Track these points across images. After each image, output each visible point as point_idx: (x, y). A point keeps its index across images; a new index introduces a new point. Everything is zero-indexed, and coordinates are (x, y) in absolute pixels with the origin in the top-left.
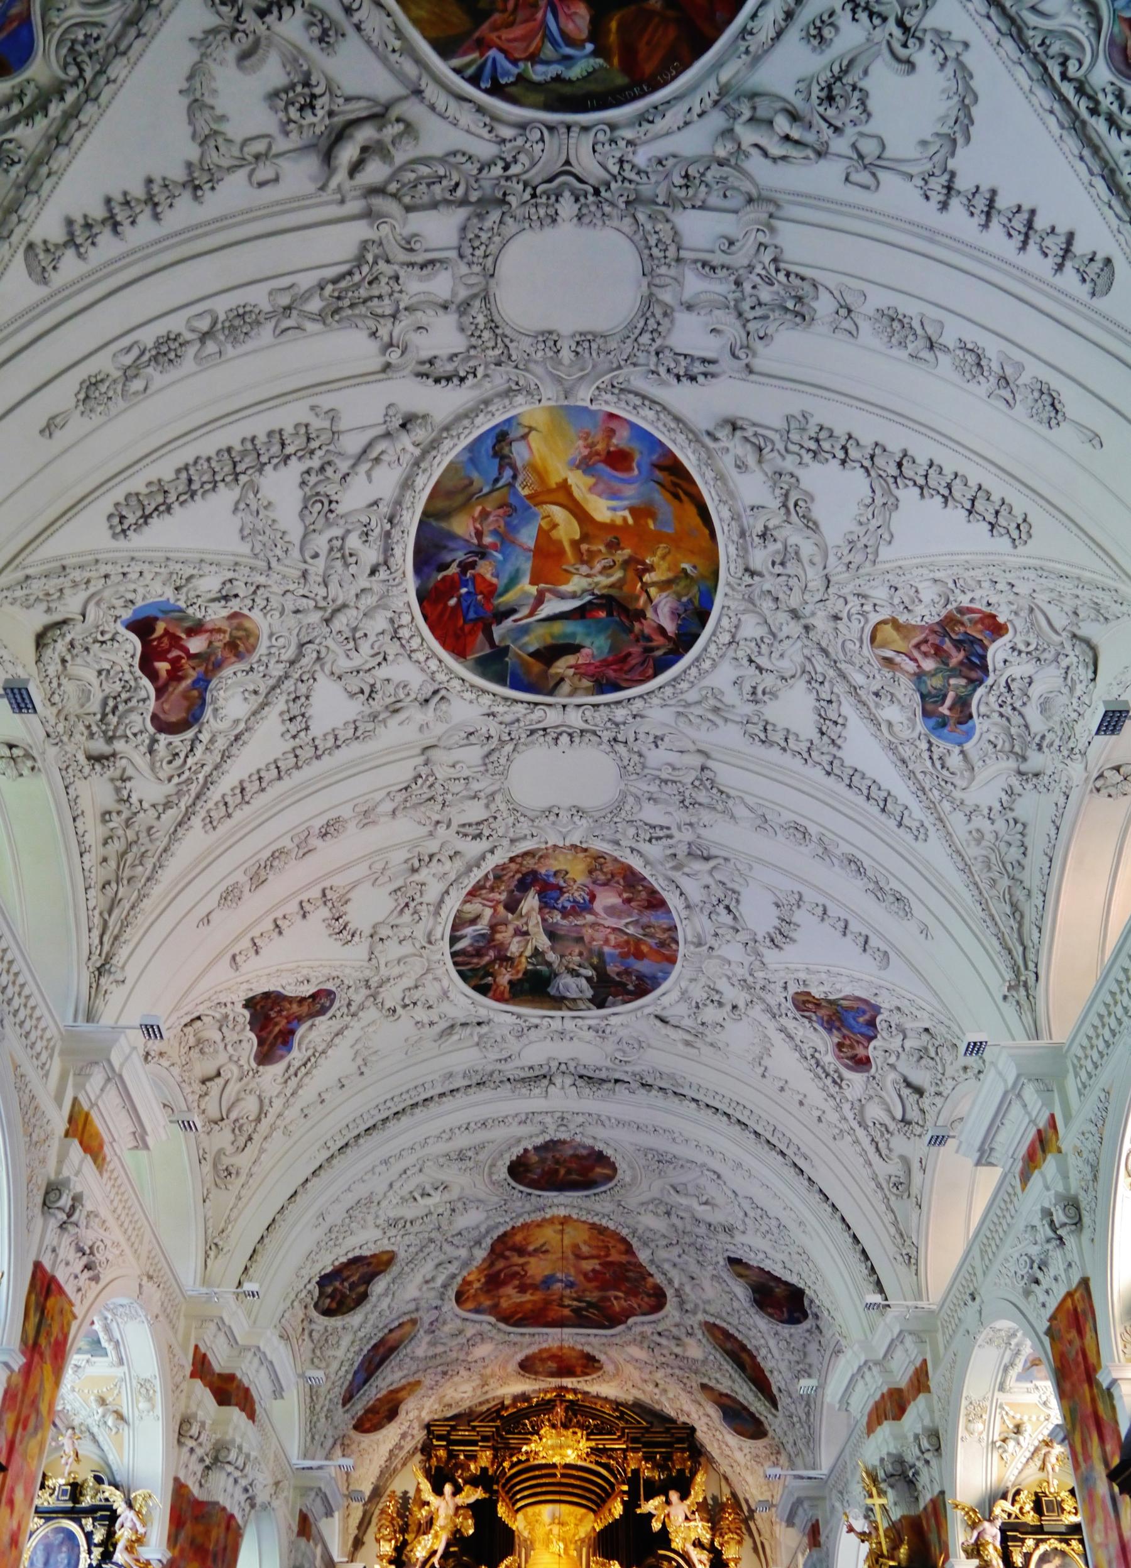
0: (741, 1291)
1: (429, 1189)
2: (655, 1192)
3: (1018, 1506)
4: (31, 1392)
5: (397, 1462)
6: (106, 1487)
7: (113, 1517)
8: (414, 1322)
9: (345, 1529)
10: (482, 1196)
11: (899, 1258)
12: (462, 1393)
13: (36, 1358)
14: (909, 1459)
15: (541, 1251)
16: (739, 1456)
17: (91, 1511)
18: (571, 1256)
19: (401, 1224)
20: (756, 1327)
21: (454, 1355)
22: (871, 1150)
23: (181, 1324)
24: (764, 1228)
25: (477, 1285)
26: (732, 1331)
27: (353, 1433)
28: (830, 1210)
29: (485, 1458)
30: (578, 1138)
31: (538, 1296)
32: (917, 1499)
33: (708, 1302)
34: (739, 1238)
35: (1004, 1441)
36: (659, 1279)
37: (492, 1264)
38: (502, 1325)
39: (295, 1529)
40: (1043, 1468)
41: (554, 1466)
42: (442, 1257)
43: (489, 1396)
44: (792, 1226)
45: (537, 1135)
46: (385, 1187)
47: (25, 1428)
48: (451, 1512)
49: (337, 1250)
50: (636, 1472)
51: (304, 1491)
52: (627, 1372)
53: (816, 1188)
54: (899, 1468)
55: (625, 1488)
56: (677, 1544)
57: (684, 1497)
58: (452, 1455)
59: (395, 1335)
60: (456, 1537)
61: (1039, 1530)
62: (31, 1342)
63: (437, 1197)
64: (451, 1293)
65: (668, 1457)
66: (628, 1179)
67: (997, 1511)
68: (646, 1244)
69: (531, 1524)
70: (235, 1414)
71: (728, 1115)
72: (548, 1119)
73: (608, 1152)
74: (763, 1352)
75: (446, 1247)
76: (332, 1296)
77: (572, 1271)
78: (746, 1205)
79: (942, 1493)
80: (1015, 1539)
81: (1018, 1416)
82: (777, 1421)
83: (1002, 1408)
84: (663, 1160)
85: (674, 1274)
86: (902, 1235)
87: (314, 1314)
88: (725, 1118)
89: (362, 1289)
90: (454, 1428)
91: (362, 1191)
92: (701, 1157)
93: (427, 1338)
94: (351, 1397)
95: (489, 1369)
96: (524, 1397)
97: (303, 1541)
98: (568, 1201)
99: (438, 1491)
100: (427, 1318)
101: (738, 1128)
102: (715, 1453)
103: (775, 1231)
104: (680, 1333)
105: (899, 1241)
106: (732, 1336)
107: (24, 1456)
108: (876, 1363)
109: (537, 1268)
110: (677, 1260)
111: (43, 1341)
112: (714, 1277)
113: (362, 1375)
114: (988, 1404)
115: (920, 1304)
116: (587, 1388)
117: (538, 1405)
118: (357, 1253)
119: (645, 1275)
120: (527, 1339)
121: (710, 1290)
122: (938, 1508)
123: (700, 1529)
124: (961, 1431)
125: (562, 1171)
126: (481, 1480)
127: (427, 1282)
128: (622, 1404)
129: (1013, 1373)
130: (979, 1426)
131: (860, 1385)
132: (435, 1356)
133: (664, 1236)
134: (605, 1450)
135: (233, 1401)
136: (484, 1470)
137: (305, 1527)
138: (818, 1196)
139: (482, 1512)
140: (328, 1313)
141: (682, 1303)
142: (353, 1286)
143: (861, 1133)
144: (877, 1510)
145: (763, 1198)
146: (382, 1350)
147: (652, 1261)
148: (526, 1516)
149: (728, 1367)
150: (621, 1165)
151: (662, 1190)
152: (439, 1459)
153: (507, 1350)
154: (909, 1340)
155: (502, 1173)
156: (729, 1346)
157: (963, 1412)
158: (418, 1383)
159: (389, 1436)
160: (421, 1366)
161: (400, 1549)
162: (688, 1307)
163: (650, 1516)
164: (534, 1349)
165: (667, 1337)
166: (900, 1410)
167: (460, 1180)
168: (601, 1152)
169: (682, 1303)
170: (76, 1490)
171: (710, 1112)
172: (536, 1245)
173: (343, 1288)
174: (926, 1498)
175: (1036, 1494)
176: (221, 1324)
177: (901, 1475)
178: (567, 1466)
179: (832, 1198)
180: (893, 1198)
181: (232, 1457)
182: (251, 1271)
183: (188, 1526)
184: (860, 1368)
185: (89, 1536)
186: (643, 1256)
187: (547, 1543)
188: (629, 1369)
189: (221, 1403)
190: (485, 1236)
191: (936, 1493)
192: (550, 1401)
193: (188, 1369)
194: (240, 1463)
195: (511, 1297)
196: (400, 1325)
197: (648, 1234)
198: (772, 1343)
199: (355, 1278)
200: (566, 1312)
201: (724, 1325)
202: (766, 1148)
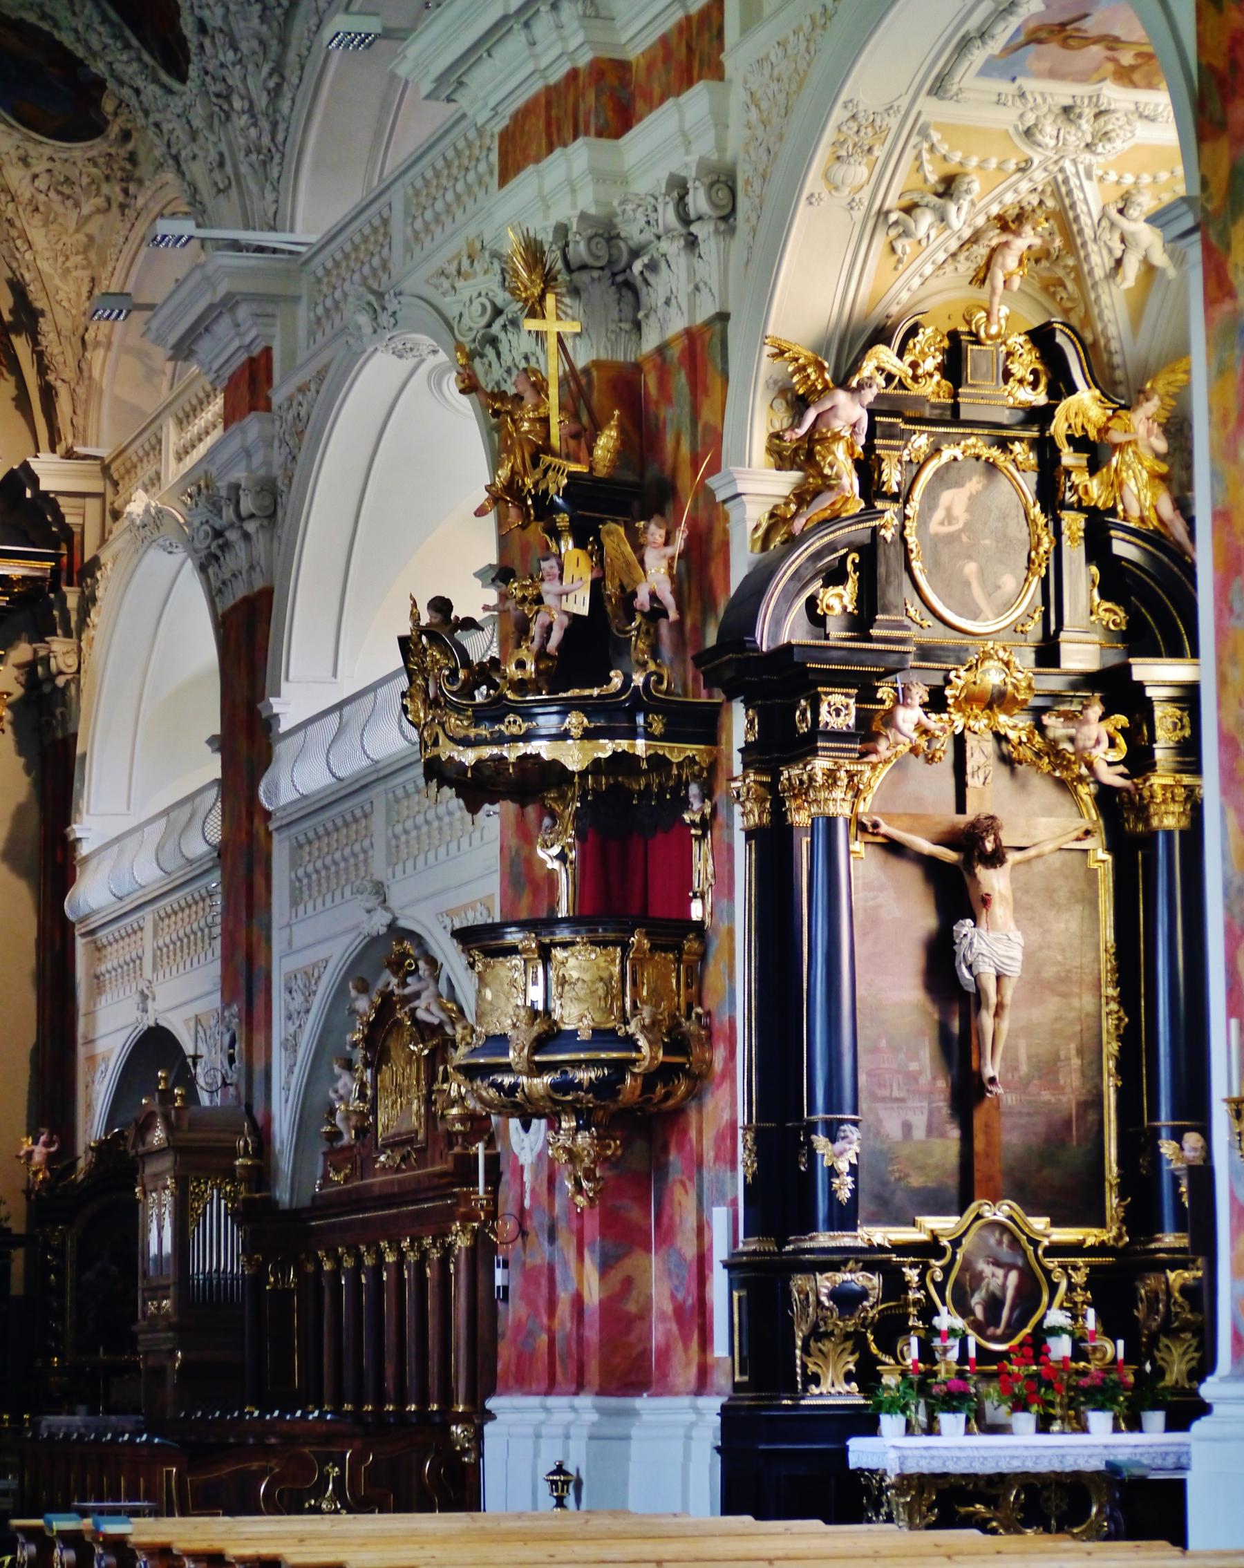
3: (908, 358)
14: (633, 231)
32: (638, 326)
35: (909, 210)
40: (982, 277)
54: (602, 251)
61: (952, 416)
67: (868, 368)
79: (723, 317)
80: (891, 432)
81: (957, 157)
82: (177, 105)
83: (924, 134)
114: (893, 122)
122: (703, 355)
124: (813, 182)
129: (978, 56)
130: (859, 172)
131: (515, 43)
144: (552, 342)
157: (829, 135)
166: (620, 120)
174: (666, 324)
175: (953, 335)
177: (606, 269)
191: (702, 316)
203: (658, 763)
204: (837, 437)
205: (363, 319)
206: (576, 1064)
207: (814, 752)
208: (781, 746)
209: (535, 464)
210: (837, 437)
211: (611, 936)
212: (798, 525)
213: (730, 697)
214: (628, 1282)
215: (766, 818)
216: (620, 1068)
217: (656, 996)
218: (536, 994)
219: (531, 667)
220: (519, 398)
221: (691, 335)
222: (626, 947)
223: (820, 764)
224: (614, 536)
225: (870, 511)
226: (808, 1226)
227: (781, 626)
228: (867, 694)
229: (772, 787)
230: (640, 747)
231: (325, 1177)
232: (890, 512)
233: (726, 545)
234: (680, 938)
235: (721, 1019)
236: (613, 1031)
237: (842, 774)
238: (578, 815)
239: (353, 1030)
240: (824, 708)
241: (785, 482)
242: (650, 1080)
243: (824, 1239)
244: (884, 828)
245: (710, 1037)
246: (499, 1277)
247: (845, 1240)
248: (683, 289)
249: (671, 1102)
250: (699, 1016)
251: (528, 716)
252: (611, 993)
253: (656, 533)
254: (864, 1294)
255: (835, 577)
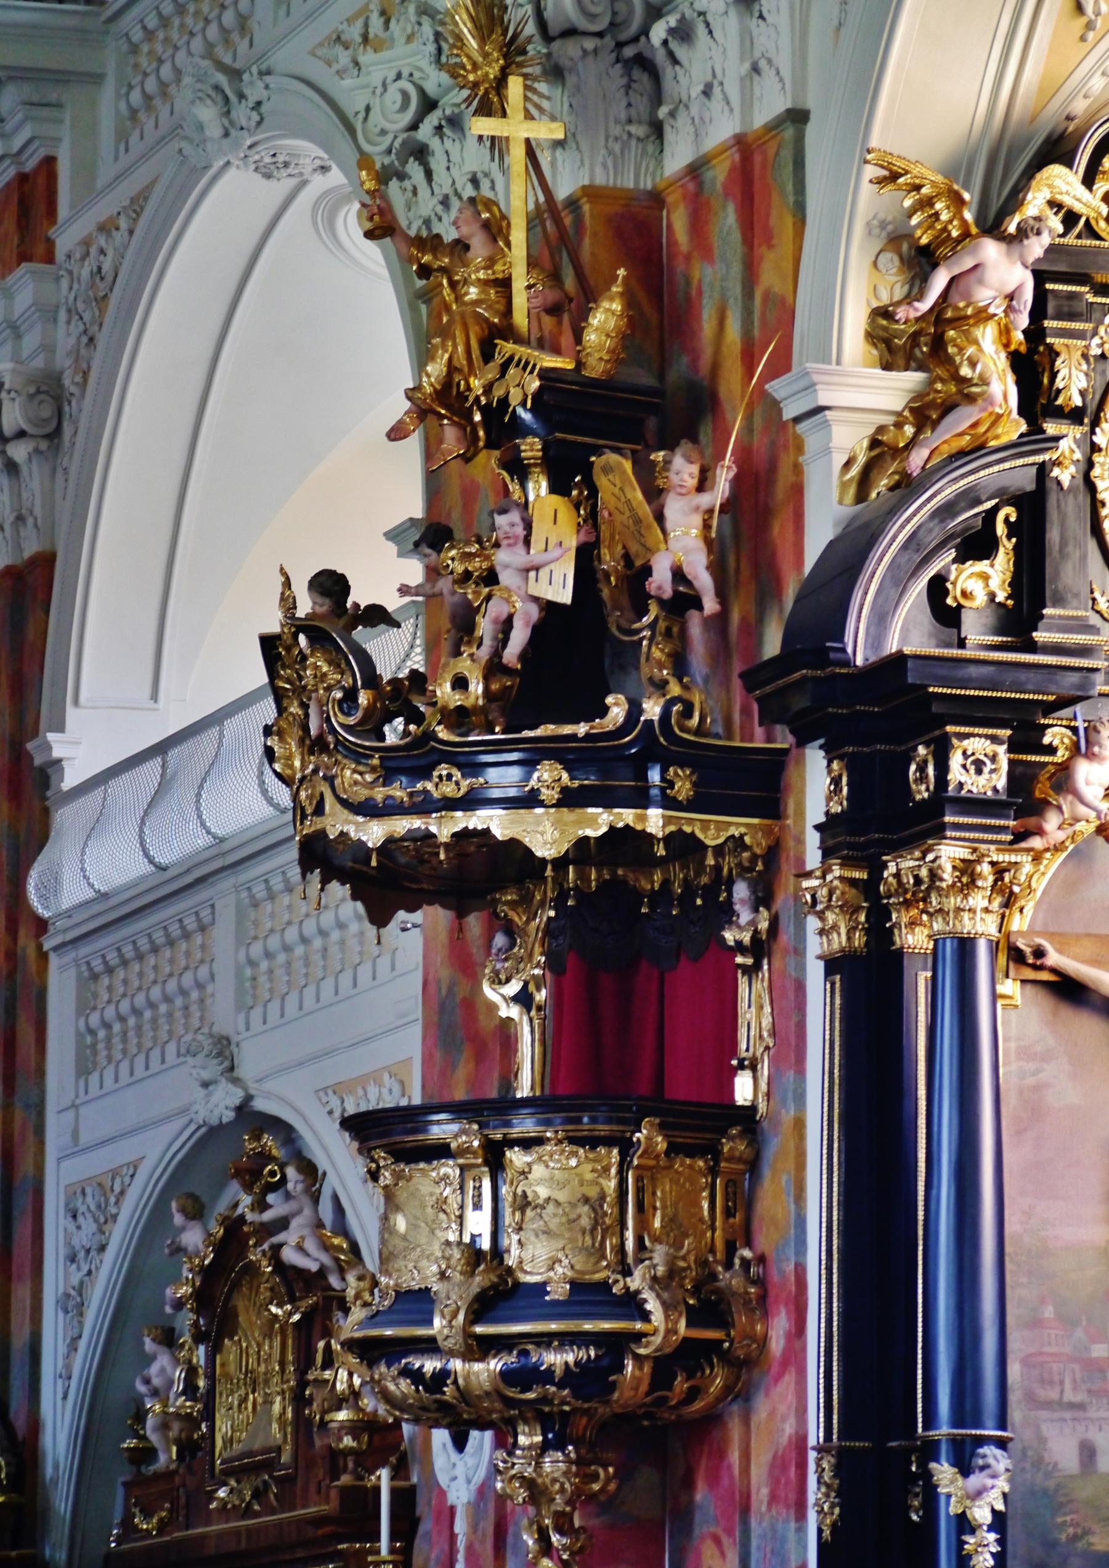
32: (657, 130)
67: (1035, 203)
79: (798, 117)
122: (763, 176)
144: (517, 154)
174: (704, 130)
203: (683, 846)
204: (983, 316)
205: (208, 114)
206: (544, 1340)
207: (939, 832)
208: (885, 820)
209: (487, 355)
210: (983, 316)
211: (603, 1129)
212: (917, 460)
213: (802, 741)
215: (859, 940)
216: (615, 1347)
217: (675, 1230)
218: (479, 1223)
219: (477, 688)
220: (461, 246)
221: (745, 146)
222: (626, 1147)
223: (949, 853)
224: (615, 473)
225: (1035, 437)
227: (886, 626)
228: (1026, 738)
229: (869, 889)
230: (654, 820)
231: (127, 1523)
232: (1069, 440)
233: (798, 491)
234: (718, 1135)
235: (782, 1269)
236: (604, 1286)
237: (985, 868)
238: (550, 931)
239: (176, 1280)
240: (956, 760)
241: (896, 389)
242: (663, 1367)
244: (1053, 958)
245: (763, 1297)
248: (733, 70)
249: (698, 1405)
250: (746, 1264)
251: (472, 768)
252: (601, 1221)
253: (683, 469)
255: (977, 545)
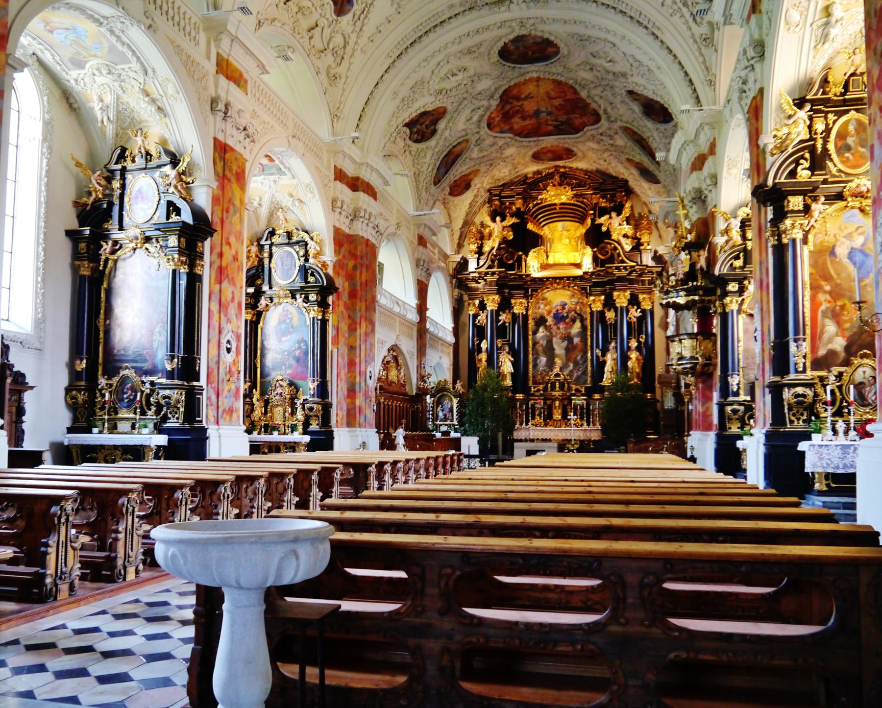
0: (636, 108)
1: (455, 71)
2: (582, 58)
4: (227, 197)
5: (475, 209)
6: (301, 232)
7: (306, 244)
8: (467, 141)
9: (452, 240)
10: (489, 72)
11: (705, 83)
12: (503, 173)
13: (226, 181)
15: (528, 97)
16: (649, 192)
17: (297, 243)
18: (547, 99)
19: (444, 93)
20: (646, 126)
21: (494, 155)
22: (691, 20)
23: (325, 156)
24: (642, 72)
25: (498, 119)
26: (635, 130)
27: (449, 197)
28: (673, 58)
29: (519, 203)
30: (533, 33)
31: (533, 121)
32: (706, 209)
33: (621, 116)
34: (631, 79)
36: (594, 106)
37: (503, 107)
38: (517, 138)
39: (416, 242)
41: (555, 204)
42: (473, 107)
43: (519, 173)
44: (655, 69)
45: (510, 34)
46: (430, 73)
47: (228, 212)
48: (501, 229)
49: (410, 110)
50: (596, 204)
51: (419, 226)
52: (589, 156)
53: (665, 46)
55: (592, 212)
56: (614, 236)
57: (619, 214)
58: (502, 203)
59: (458, 149)
60: (504, 240)
62: (221, 175)
63: (461, 76)
64: (484, 124)
65: (613, 196)
66: (566, 53)
68: (584, 88)
69: (552, 232)
70: (361, 195)
71: (614, 8)
72: (514, 24)
73: (552, 38)
74: (651, 139)
75: (474, 101)
76: (418, 132)
77: (549, 106)
78: (631, 60)
84: (583, 40)
85: (601, 102)
86: (707, 69)
87: (410, 143)
88: (613, 11)
89: (432, 128)
90: (502, 190)
91: (416, 77)
92: (603, 35)
93: (476, 149)
94: (439, 181)
95: (516, 160)
96: (538, 172)
97: (421, 248)
98: (536, 69)
99: (494, 221)
100: (473, 139)
101: (620, 15)
102: (639, 192)
103: (647, 73)
104: (612, 132)
105: (706, 73)
106: (635, 133)
107: (231, 223)
108: (691, 142)
109: (530, 106)
110: (602, 94)
111: (228, 173)
112: (622, 102)
113: (442, 170)
115: (714, 107)
116: (570, 165)
117: (546, 175)
118: (423, 110)
119: (587, 105)
120: (532, 144)
121: (622, 109)
122: (713, 216)
123: (628, 229)
125: (530, 53)
126: (518, 214)
127: (468, 120)
128: (591, 172)
131: (684, 154)
132: (484, 157)
133: (592, 82)
134: (581, 195)
135: (361, 189)
136: (518, 209)
137: (422, 241)
138: (666, 51)
139: (519, 229)
140: (417, 141)
141: (608, 118)
142: (427, 127)
143: (684, 10)
145: (640, 56)
146: (452, 157)
147: (588, 96)
148: (549, 228)
149: (637, 149)
150: (561, 45)
151: (586, 56)
152: (496, 205)
153: (523, 151)
154: (706, 128)
155: (495, 57)
156: (636, 137)
157: (725, 164)
158: (478, 170)
159: (467, 198)
160: (478, 162)
161: (480, 247)
162: (612, 119)
163: (601, 225)
164: (539, 148)
165: (606, 136)
167: (473, 65)
168: (547, 39)
169: (608, 118)
170: (289, 235)
171: (604, 7)
172: (526, 94)
173: (422, 127)
176: (345, 155)
178: (562, 204)
179: (675, 51)
180: (703, 48)
181: (362, 214)
182: (360, 126)
183: (346, 246)
184: (682, 145)
185: (297, 253)
186: (583, 94)
187: (560, 239)
188: (590, 154)
189: (354, 191)
190: (495, 93)
192: (552, 173)
193: (332, 177)
194: (367, 216)
195: (518, 123)
196: (459, 143)
197: (583, 82)
198: (655, 134)
199: (427, 123)
200: (550, 128)
201: (631, 127)
202: (637, 25)
212: (726, 248)
214: (708, 408)
216: (696, 364)
217: (705, 348)
226: (728, 396)
230: (697, 298)
242: (704, 366)
243: (731, 399)
246: (690, 407)
247: (736, 399)
252: (694, 348)
253: (702, 252)
254: (739, 410)
255: (737, 258)
